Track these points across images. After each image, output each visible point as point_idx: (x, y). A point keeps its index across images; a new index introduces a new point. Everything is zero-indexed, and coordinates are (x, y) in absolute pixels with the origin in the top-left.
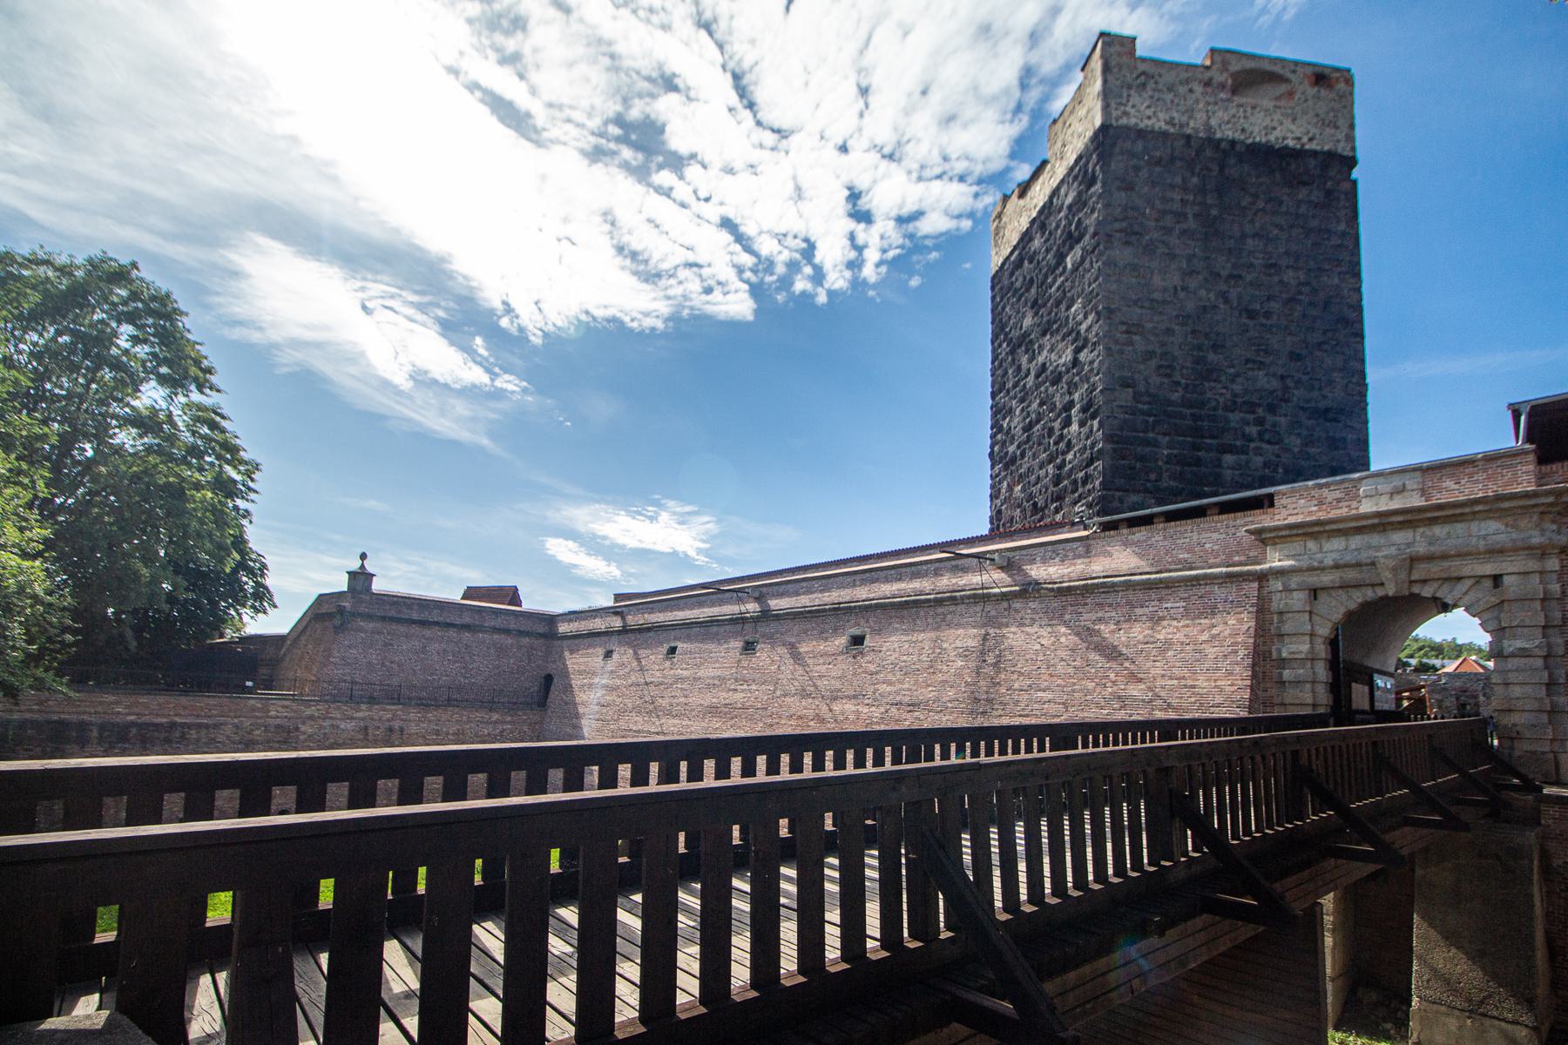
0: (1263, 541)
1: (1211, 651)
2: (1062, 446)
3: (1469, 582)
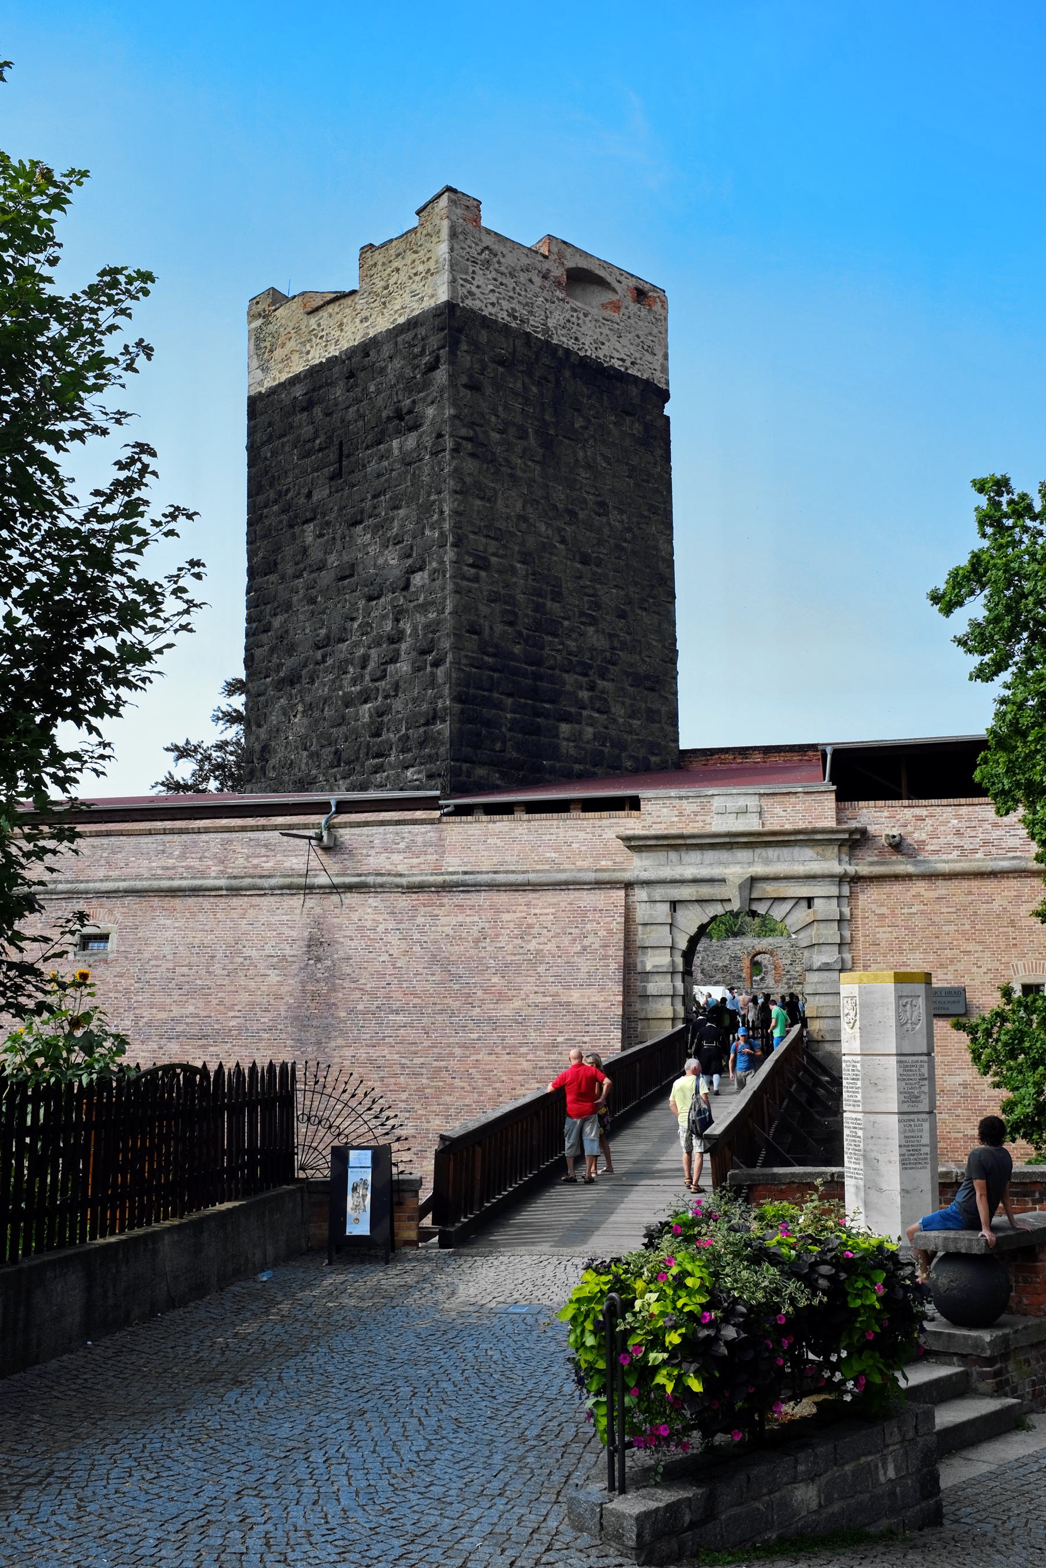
1: (584, 965)
3: (791, 903)
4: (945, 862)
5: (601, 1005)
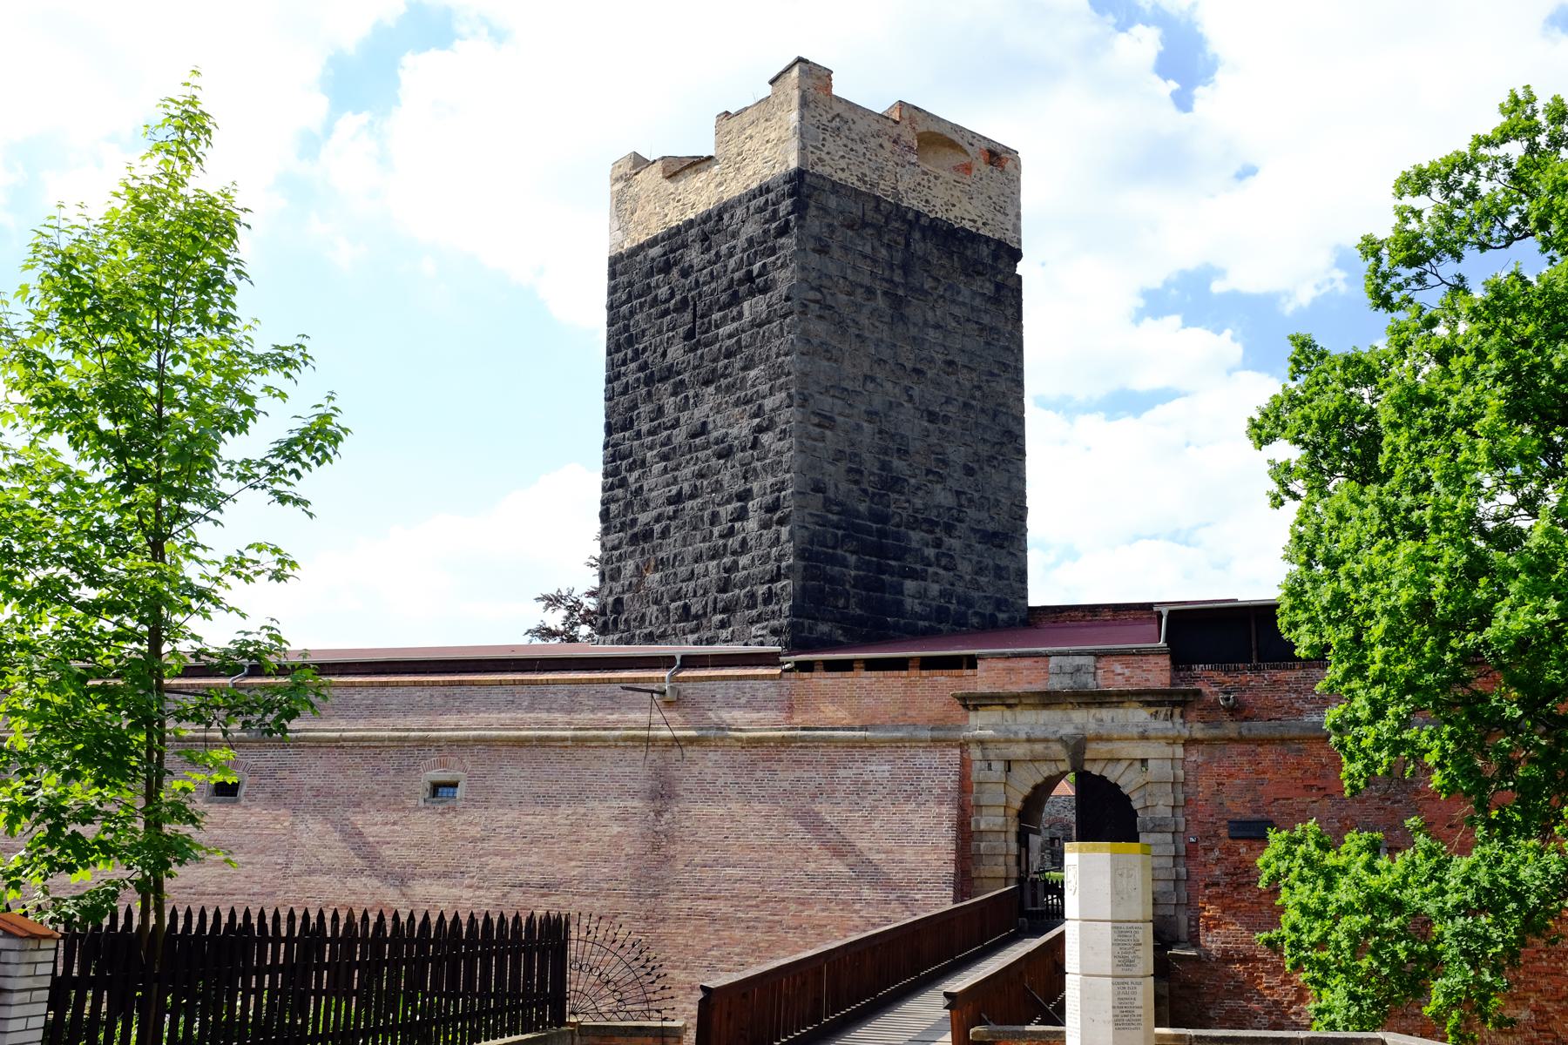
0: (966, 706)
2: (733, 543)
3: (1126, 764)
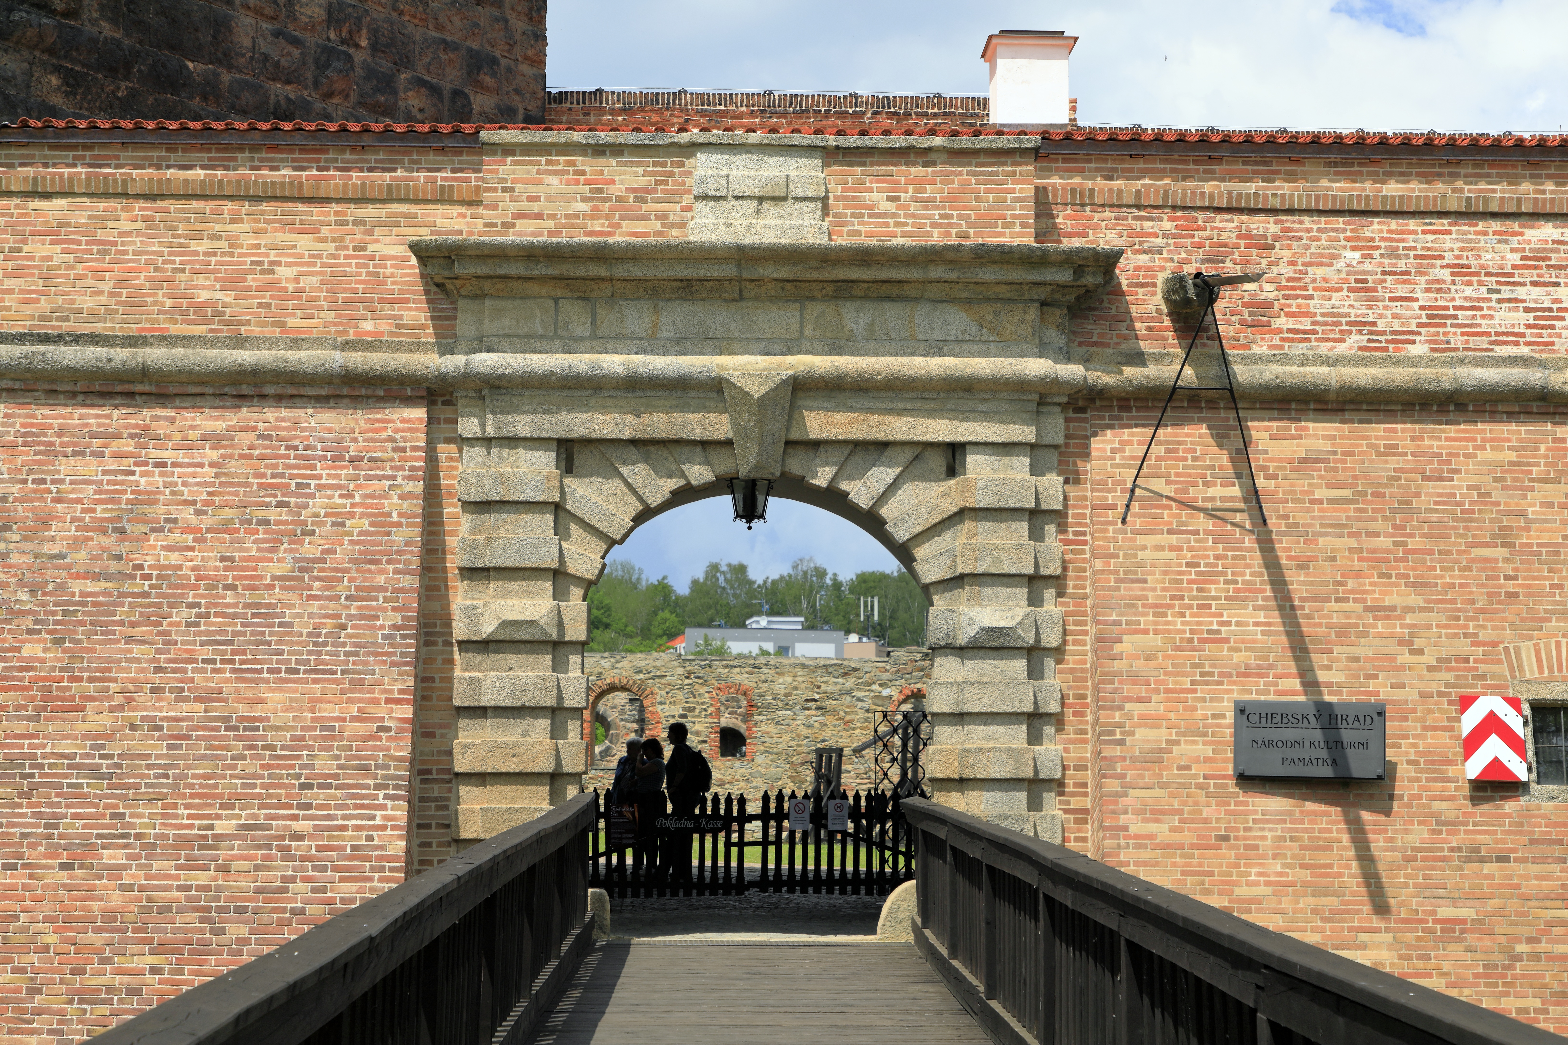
1: (302, 614)
4: (1326, 361)
5: (352, 729)
